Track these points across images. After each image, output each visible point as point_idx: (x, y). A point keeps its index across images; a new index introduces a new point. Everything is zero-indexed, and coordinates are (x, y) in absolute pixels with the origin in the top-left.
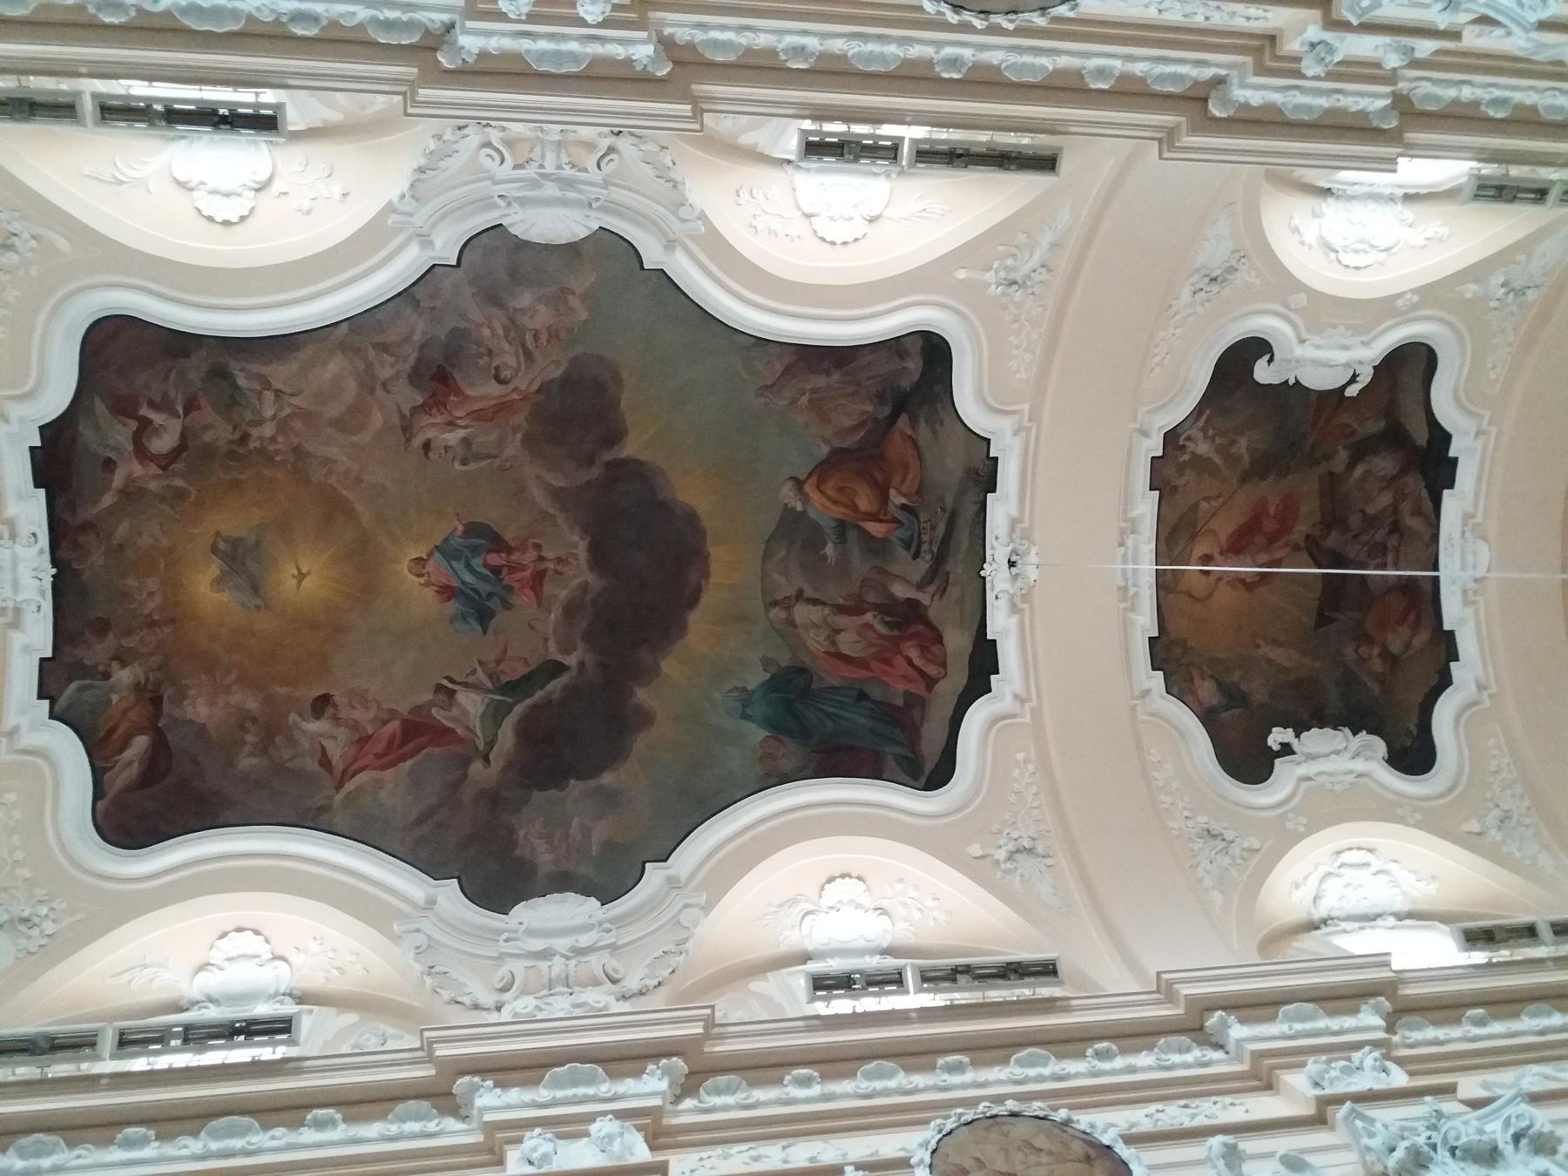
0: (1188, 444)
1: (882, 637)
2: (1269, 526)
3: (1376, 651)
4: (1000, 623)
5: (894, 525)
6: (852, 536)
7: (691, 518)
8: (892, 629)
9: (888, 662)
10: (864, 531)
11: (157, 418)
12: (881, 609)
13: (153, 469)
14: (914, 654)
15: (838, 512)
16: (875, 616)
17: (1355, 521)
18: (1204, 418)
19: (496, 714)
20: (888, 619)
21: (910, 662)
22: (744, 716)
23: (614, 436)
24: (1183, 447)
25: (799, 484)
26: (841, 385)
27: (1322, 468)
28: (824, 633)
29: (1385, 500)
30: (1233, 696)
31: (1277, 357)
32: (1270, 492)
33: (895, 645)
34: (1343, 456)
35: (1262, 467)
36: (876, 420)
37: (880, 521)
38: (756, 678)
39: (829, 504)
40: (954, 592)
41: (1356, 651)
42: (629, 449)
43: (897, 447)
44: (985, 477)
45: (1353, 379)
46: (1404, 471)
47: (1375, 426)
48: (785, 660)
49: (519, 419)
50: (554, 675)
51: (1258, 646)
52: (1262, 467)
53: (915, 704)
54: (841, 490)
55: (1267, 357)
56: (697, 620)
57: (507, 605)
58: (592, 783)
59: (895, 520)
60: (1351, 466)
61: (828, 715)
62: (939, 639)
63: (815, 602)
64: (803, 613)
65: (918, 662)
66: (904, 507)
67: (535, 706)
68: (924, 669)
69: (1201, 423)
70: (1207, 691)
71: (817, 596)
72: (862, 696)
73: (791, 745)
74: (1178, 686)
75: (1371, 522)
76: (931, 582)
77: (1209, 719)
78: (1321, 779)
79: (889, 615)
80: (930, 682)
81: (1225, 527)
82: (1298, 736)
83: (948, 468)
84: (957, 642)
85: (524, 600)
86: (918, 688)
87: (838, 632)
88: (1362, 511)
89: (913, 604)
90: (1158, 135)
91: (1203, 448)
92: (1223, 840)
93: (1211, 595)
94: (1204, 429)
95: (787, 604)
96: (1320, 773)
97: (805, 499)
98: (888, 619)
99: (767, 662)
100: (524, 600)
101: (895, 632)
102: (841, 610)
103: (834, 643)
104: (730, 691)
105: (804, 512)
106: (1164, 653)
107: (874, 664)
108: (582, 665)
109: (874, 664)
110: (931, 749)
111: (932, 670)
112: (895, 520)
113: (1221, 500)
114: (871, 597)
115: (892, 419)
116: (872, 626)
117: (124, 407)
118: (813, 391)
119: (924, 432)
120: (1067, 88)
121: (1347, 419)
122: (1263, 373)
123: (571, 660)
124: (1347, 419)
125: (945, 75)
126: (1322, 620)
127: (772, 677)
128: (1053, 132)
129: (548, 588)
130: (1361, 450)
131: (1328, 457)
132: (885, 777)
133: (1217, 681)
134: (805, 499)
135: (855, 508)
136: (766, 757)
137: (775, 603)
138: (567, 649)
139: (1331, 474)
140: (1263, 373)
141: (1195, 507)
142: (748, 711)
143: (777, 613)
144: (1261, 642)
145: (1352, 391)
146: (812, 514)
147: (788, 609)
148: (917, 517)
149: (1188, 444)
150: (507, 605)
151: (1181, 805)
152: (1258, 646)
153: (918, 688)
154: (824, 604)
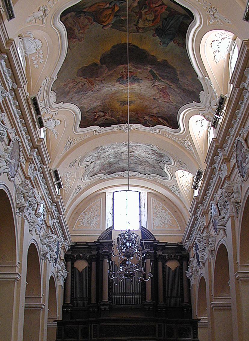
1: (149, 10)
5: (115, 6)
6: (118, 14)
8: (147, 8)
9: (156, 11)
10: (117, 12)
12: (141, 9)
14: (154, 5)
15: (112, 17)
16: (143, 10)
20: (144, 8)
22: (168, 44)
25: (104, 26)
26: (77, 26)
28: (146, 22)
37: (114, 8)
38: (158, 39)
39: (110, 19)
54: (105, 17)
56: (142, 47)
59: (114, 6)
61: (169, 28)
63: (138, 22)
64: (141, 25)
68: (159, 5)
71: (136, 22)
72: (166, 19)
79: (142, 7)
87: (147, 19)
95: (138, 29)
97: (109, 24)
98: (144, 8)
99: (153, 35)
102: (140, 17)
103: (150, 20)
104: (161, 45)
105: (112, 24)
109: (157, 14)
112: (114, 6)
114: (137, 10)
116: (146, 12)
127: (158, 36)
132: (188, 24)
134: (109, 24)
135: (111, 13)
136: (179, 44)
142: (166, 43)
143: (140, 31)
147: (140, 28)
154: (138, 20)
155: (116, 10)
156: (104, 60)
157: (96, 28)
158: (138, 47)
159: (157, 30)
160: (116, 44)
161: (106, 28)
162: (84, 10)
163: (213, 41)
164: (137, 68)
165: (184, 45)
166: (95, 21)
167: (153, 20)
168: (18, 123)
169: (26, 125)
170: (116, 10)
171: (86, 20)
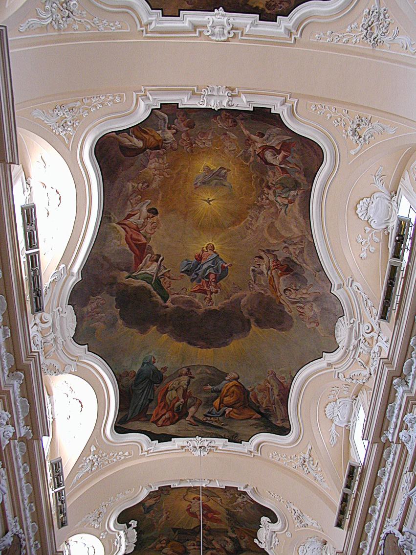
0: (241, 497)
1: (174, 405)
2: (210, 515)
3: (164, 545)
4: (177, 442)
5: (218, 408)
6: (214, 394)
7: (226, 344)
8: (177, 407)
9: (164, 407)
10: (216, 398)
11: (280, 157)
13: (258, 151)
14: (167, 416)
16: (182, 402)
17: (211, 537)
18: (250, 502)
19: (147, 278)
20: (181, 406)
21: (164, 414)
22: (143, 364)
23: (259, 323)
24: (240, 496)
25: (236, 379)
26: (273, 398)
27: (229, 529)
29: (217, 546)
30: (148, 510)
31: (270, 524)
32: (223, 516)
33: (172, 410)
34: (234, 536)
35: (231, 515)
36: (259, 407)
37: (220, 404)
38: (158, 365)
39: (227, 388)
40: (191, 428)
41: (164, 540)
42: (254, 327)
43: (248, 412)
44: (234, 438)
45: (260, 542)
46: (227, 552)
47: (243, 546)
48: (166, 374)
49: (269, 293)
50: (162, 297)
51: (166, 513)
52: (231, 515)
53: (147, 419)
54: (233, 392)
55: (270, 522)
56: (183, 345)
57: (192, 280)
58: (118, 317)
60: (230, 538)
61: (144, 391)
62: (172, 423)
63: (189, 382)
64: (184, 380)
65: (164, 417)
66: (225, 412)
67: (150, 291)
68: (161, 419)
69: (248, 501)
70: (152, 502)
71: (191, 383)
72: (151, 401)
73: (132, 381)
74: (151, 495)
75: (210, 542)
76: (195, 420)
77: (142, 503)
78: (118, 538)
79: (182, 407)
80: (155, 422)
81: (210, 504)
82: (134, 528)
83: (238, 428)
84: (171, 429)
85: (195, 286)
86: (153, 418)
87: (176, 390)
88: (213, 539)
89: (187, 414)
90: (344, 552)
91: (239, 500)
92: (98, 518)
93: (185, 500)
94: (246, 501)
96: (120, 537)
97: (230, 381)
98: (181, 406)
99: (165, 369)
100: (195, 286)
101: (175, 409)
102: (185, 391)
103: (172, 390)
104: (154, 358)
105: (225, 380)
106: (165, 490)
107: (163, 403)
108: (167, 307)
110: (129, 426)
111: (160, 422)
112: (220, 409)
113: (220, 503)
115: (260, 413)
116: (178, 401)
117: (285, 146)
118: (272, 389)
119: (253, 422)
120: (362, 536)
121: (247, 538)
122: (264, 519)
123: (168, 303)
124: (247, 538)
125: (370, 509)
126: (175, 530)
127: (159, 371)
128: (349, 527)
129: (199, 295)
130: (235, 541)
131: (234, 532)
133: (154, 504)
134: (230, 381)
135: (225, 397)
136: (127, 374)
137: (189, 370)
138: (173, 302)
139: (227, 532)
140: (264, 519)
141: (219, 497)
142: (145, 365)
144: (168, 513)
145: (256, 541)
146: (224, 382)
147: (186, 374)
148: (220, 416)
149: (241, 497)
150: (192, 280)
151: (110, 502)
152: (166, 513)
153: (153, 418)
154: (188, 386)
155: (218, 401)
156: (245, 327)
157: (251, 381)
158: (190, 343)
159: (161, 379)
160: (222, 348)
161: (234, 375)
162: (259, 416)
163: (82, 406)
164: (190, 303)
165: (119, 378)
166: (248, 392)
167: (167, 391)
168: (377, 522)
169: (376, 481)
170: (218, 401)
171: (259, 398)
